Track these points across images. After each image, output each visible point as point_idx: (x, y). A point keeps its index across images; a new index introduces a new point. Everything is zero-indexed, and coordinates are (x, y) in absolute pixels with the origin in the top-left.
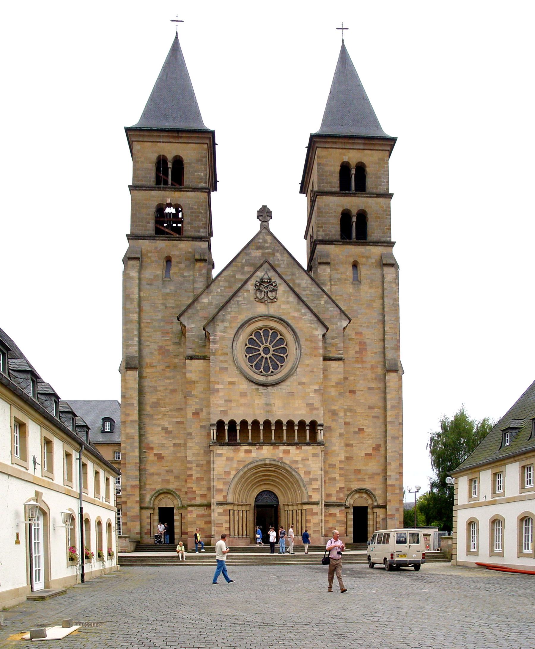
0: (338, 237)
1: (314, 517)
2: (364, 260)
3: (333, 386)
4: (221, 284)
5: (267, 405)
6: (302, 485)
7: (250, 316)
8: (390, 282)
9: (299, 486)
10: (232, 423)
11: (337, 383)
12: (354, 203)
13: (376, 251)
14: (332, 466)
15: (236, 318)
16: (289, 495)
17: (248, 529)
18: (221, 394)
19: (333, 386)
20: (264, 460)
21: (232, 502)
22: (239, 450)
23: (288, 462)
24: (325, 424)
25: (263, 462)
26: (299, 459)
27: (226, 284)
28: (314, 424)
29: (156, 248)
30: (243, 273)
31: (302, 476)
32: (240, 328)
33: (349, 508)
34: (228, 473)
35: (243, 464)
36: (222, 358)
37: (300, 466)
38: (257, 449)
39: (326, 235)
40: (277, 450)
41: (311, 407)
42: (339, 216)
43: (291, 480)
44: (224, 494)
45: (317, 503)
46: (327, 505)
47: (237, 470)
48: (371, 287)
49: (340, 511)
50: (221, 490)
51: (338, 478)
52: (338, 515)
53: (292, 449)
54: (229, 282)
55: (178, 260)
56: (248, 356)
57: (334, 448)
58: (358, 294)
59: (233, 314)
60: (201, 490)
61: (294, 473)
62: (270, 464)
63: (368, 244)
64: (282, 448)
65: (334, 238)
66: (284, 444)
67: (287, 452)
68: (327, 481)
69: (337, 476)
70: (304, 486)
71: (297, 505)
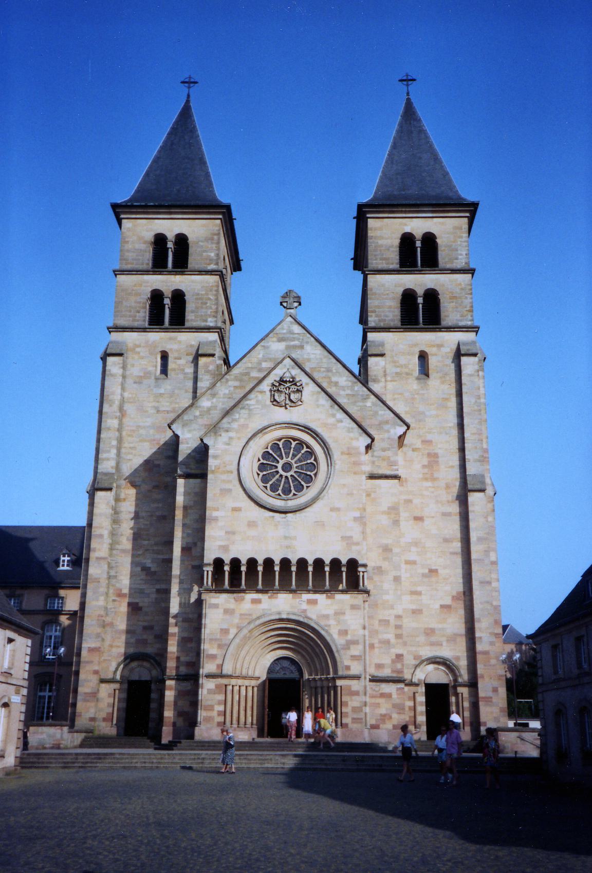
0: (398, 323)
1: (354, 698)
2: (434, 350)
3: (383, 513)
4: (230, 383)
5: (286, 538)
7: (266, 423)
8: (471, 375)
10: (235, 562)
11: (389, 508)
12: (420, 282)
13: (451, 339)
14: (385, 623)
15: (245, 426)
18: (220, 524)
19: (383, 513)
20: (279, 613)
22: (243, 599)
23: (314, 617)
24: (371, 564)
26: (330, 611)
27: (237, 384)
28: (353, 564)
29: (147, 342)
30: (260, 370)
31: (336, 636)
32: (254, 435)
33: (417, 685)
34: (225, 631)
36: (224, 477)
37: (332, 622)
38: (269, 598)
39: (380, 321)
40: (298, 600)
41: (347, 540)
42: (399, 296)
44: (219, 661)
45: (357, 677)
46: (375, 680)
48: (443, 383)
49: (398, 689)
50: (214, 657)
51: (393, 641)
52: (394, 696)
53: (321, 598)
54: (241, 381)
55: (176, 355)
56: (261, 474)
57: (385, 597)
58: (425, 392)
59: (242, 421)
60: (187, 655)
63: (440, 330)
64: (306, 596)
65: (392, 324)
66: (309, 591)
67: (314, 602)
68: (376, 645)
69: (390, 636)
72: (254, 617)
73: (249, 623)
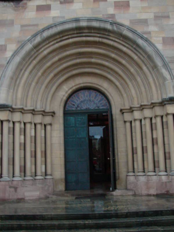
6: (159, 63)
9: (155, 67)
16: (133, 91)
17: (49, 160)
20: (77, 20)
21: (9, 103)
23: (127, 23)
25: (73, 25)
26: (149, 15)
31: (160, 46)
35: (33, 30)
37: (152, 28)
43: (135, 57)
47: (18, 42)
61: (140, 42)
62: (89, 28)
70: (165, 65)
71: (153, 105)
72: (41, 28)
73: (35, 36)
